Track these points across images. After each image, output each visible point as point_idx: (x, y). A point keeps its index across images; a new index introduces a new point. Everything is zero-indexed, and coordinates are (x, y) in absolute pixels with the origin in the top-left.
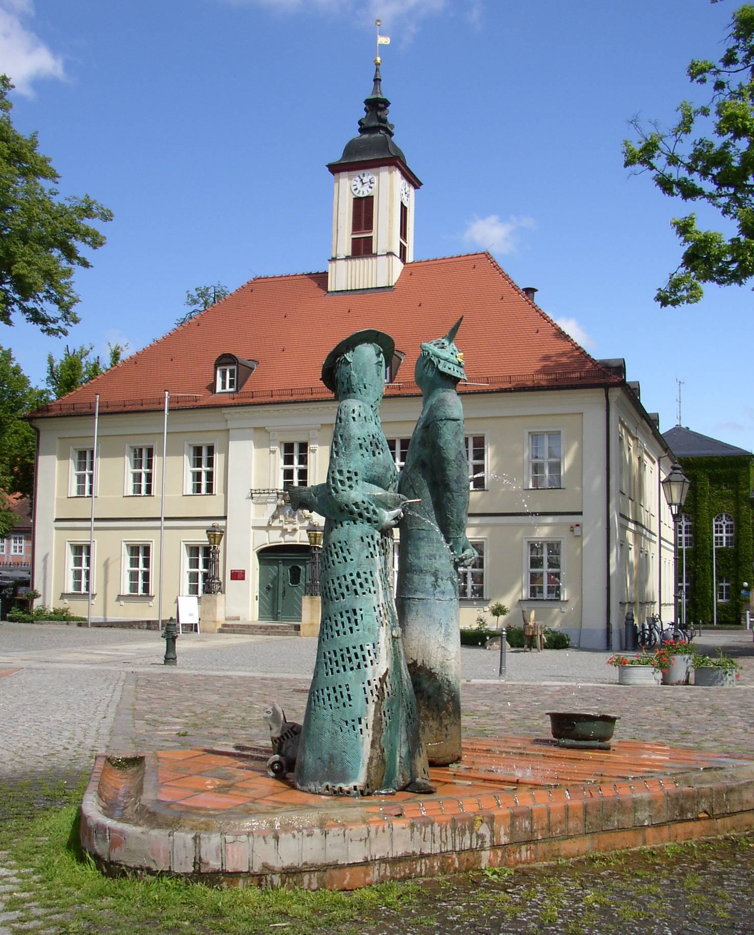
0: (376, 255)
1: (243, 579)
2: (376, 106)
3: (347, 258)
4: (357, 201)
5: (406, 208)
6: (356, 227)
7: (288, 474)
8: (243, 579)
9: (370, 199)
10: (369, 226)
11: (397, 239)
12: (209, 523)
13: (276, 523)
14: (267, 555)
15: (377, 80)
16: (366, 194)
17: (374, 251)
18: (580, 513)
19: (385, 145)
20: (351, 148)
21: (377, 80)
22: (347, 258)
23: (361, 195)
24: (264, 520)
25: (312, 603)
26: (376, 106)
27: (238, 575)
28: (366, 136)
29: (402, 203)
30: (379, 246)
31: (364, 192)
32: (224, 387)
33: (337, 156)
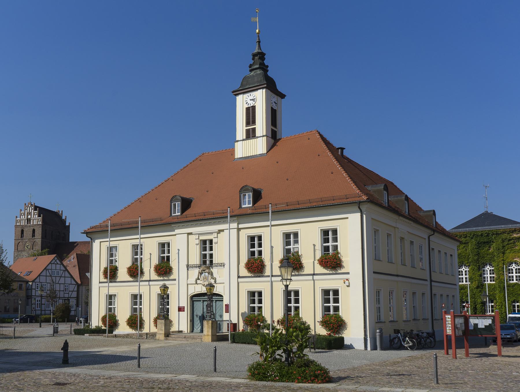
1: (184, 311)
3: (243, 140)
4: (248, 109)
5: (276, 110)
6: (248, 124)
7: (205, 256)
8: (184, 311)
9: (254, 108)
10: (254, 122)
12: (162, 283)
13: (198, 282)
14: (194, 298)
22: (243, 140)
23: (249, 106)
24: (192, 280)
25: (208, 323)
27: (181, 309)
28: (252, 73)
29: (272, 108)
30: (258, 133)
31: (251, 103)
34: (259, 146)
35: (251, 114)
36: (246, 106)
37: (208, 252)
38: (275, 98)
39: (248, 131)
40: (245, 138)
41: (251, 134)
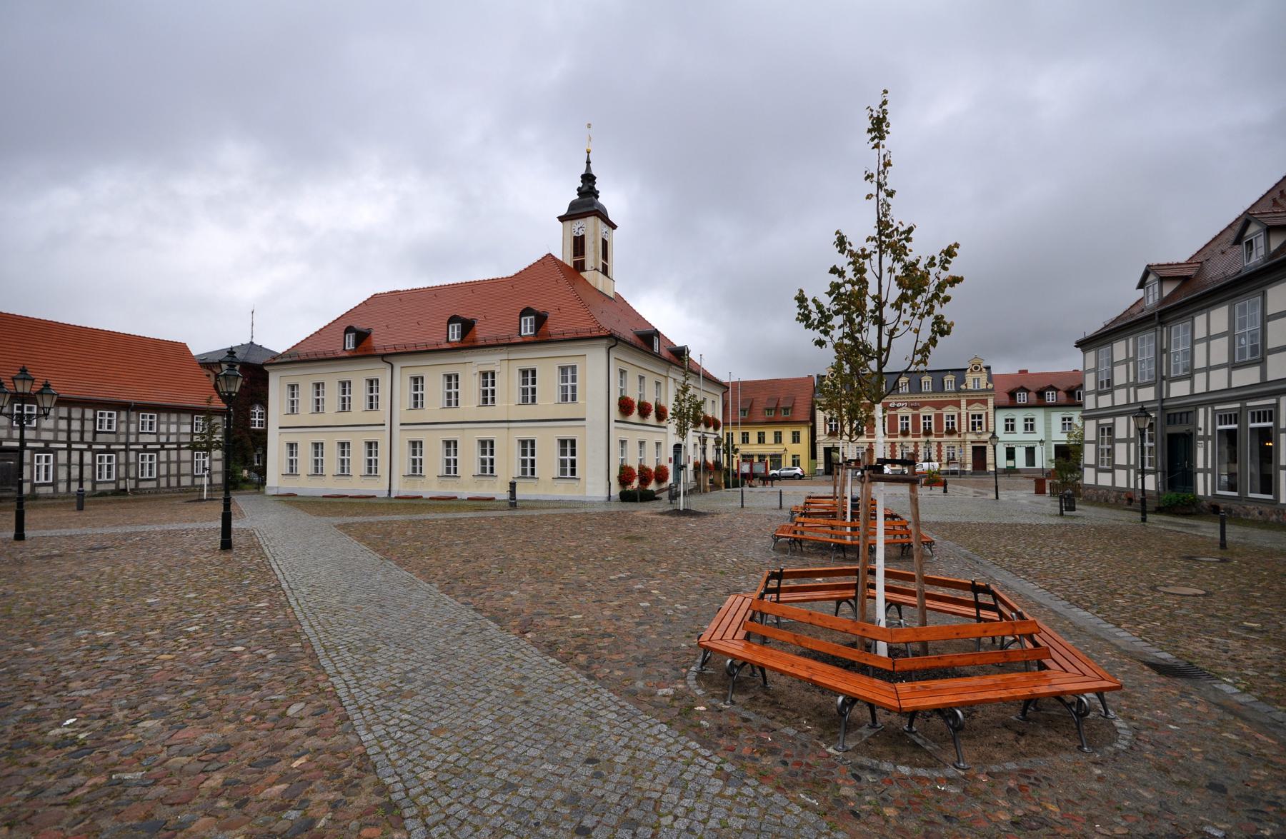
2: (588, 178)
4: (575, 238)
6: (575, 255)
10: (583, 254)
11: (601, 260)
15: (588, 162)
19: (593, 204)
20: (573, 205)
21: (588, 162)
26: (588, 178)
33: (564, 211)
38: (606, 228)
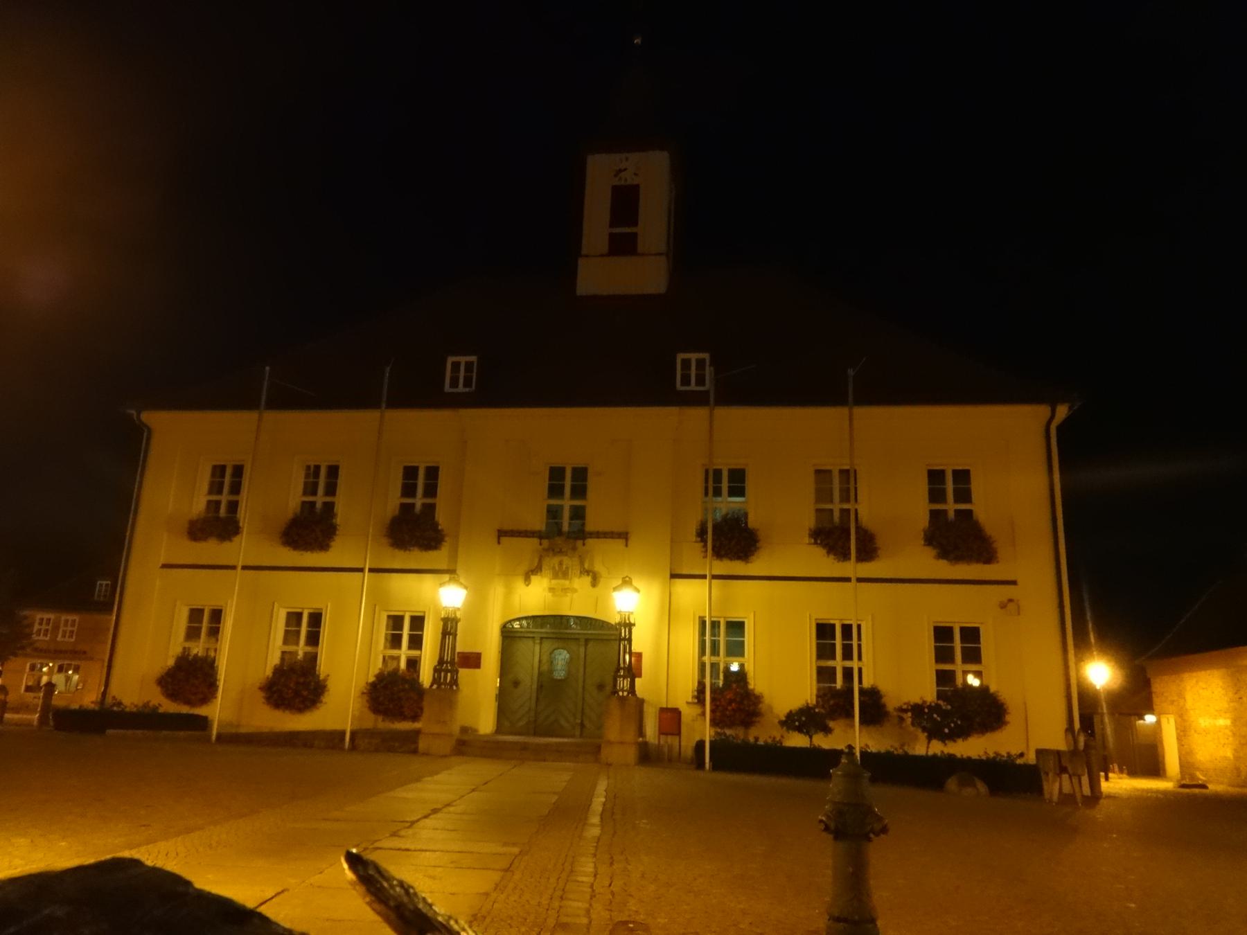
0: (643, 255)
16: (629, 182)
17: (640, 249)
18: (1014, 583)
22: (602, 255)
31: (628, 178)
32: (454, 383)
34: (646, 275)
35: (625, 203)
36: (616, 182)
37: (567, 503)
39: (613, 238)
40: (605, 249)
41: (623, 246)
